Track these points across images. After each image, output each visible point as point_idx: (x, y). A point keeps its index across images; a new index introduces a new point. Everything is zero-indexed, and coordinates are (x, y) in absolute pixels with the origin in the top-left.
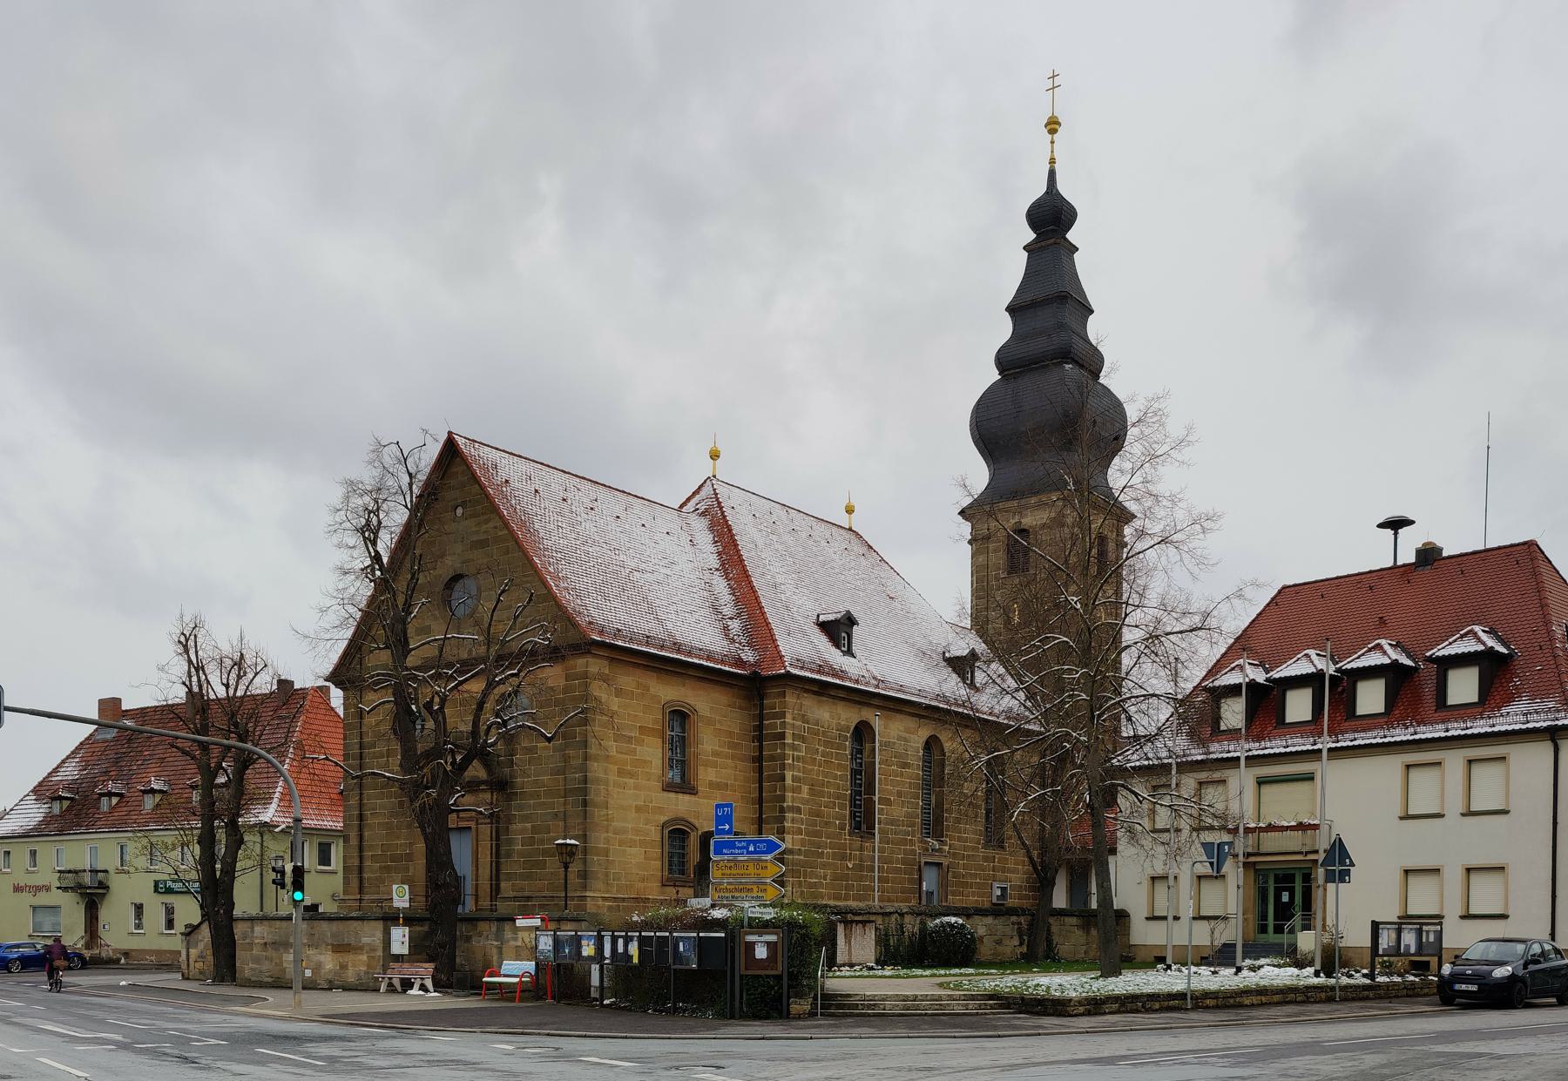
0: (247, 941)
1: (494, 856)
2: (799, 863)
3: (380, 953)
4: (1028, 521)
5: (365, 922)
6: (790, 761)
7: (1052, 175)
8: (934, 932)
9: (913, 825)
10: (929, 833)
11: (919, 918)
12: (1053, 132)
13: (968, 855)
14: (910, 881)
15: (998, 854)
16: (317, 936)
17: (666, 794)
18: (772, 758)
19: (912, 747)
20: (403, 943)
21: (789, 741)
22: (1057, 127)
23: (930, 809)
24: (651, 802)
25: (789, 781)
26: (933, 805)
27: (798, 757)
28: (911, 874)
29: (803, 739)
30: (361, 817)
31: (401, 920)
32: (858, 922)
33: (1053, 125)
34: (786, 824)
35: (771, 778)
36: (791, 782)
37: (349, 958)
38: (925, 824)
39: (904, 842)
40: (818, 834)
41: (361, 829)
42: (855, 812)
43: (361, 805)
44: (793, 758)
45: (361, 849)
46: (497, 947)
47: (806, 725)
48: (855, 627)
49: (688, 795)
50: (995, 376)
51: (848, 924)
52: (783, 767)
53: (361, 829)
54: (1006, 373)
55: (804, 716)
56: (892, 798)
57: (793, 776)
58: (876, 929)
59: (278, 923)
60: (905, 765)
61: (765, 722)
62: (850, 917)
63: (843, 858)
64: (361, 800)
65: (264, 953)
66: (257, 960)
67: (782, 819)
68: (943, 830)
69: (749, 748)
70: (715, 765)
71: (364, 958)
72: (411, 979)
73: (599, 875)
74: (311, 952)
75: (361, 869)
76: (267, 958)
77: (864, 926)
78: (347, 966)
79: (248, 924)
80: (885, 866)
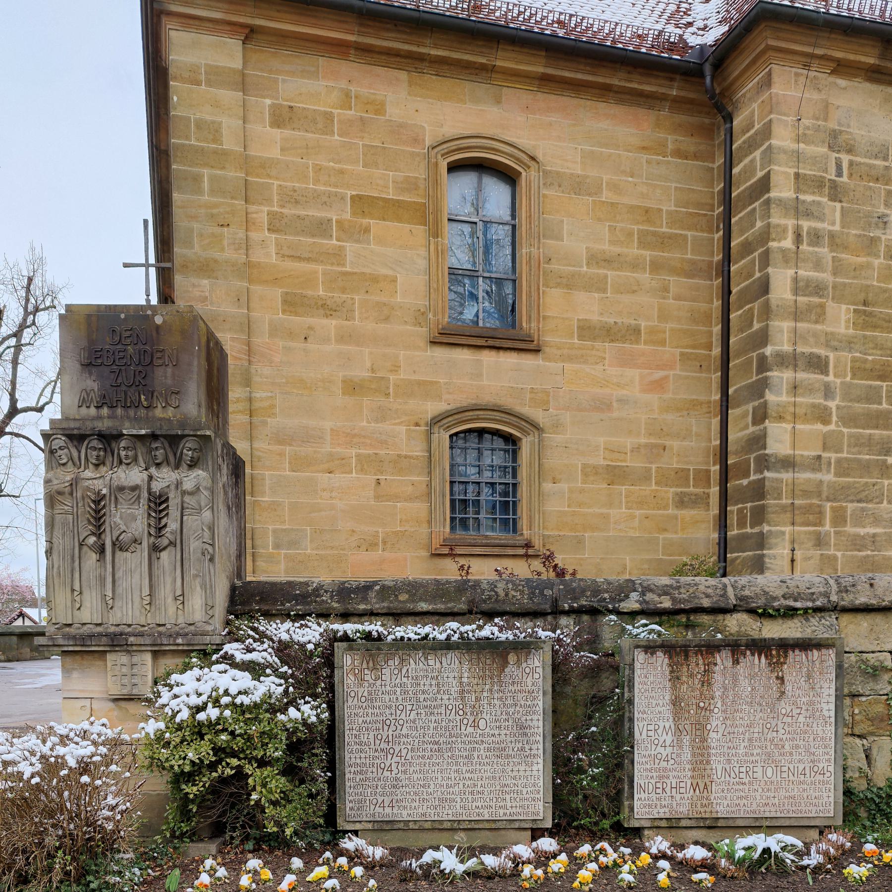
2: (817, 490)
6: (788, 243)
24: (395, 369)
27: (816, 237)
29: (836, 193)
32: (760, 647)
36: (789, 296)
47: (845, 158)
55: (834, 134)
57: (796, 280)
67: (759, 388)
70: (598, 285)
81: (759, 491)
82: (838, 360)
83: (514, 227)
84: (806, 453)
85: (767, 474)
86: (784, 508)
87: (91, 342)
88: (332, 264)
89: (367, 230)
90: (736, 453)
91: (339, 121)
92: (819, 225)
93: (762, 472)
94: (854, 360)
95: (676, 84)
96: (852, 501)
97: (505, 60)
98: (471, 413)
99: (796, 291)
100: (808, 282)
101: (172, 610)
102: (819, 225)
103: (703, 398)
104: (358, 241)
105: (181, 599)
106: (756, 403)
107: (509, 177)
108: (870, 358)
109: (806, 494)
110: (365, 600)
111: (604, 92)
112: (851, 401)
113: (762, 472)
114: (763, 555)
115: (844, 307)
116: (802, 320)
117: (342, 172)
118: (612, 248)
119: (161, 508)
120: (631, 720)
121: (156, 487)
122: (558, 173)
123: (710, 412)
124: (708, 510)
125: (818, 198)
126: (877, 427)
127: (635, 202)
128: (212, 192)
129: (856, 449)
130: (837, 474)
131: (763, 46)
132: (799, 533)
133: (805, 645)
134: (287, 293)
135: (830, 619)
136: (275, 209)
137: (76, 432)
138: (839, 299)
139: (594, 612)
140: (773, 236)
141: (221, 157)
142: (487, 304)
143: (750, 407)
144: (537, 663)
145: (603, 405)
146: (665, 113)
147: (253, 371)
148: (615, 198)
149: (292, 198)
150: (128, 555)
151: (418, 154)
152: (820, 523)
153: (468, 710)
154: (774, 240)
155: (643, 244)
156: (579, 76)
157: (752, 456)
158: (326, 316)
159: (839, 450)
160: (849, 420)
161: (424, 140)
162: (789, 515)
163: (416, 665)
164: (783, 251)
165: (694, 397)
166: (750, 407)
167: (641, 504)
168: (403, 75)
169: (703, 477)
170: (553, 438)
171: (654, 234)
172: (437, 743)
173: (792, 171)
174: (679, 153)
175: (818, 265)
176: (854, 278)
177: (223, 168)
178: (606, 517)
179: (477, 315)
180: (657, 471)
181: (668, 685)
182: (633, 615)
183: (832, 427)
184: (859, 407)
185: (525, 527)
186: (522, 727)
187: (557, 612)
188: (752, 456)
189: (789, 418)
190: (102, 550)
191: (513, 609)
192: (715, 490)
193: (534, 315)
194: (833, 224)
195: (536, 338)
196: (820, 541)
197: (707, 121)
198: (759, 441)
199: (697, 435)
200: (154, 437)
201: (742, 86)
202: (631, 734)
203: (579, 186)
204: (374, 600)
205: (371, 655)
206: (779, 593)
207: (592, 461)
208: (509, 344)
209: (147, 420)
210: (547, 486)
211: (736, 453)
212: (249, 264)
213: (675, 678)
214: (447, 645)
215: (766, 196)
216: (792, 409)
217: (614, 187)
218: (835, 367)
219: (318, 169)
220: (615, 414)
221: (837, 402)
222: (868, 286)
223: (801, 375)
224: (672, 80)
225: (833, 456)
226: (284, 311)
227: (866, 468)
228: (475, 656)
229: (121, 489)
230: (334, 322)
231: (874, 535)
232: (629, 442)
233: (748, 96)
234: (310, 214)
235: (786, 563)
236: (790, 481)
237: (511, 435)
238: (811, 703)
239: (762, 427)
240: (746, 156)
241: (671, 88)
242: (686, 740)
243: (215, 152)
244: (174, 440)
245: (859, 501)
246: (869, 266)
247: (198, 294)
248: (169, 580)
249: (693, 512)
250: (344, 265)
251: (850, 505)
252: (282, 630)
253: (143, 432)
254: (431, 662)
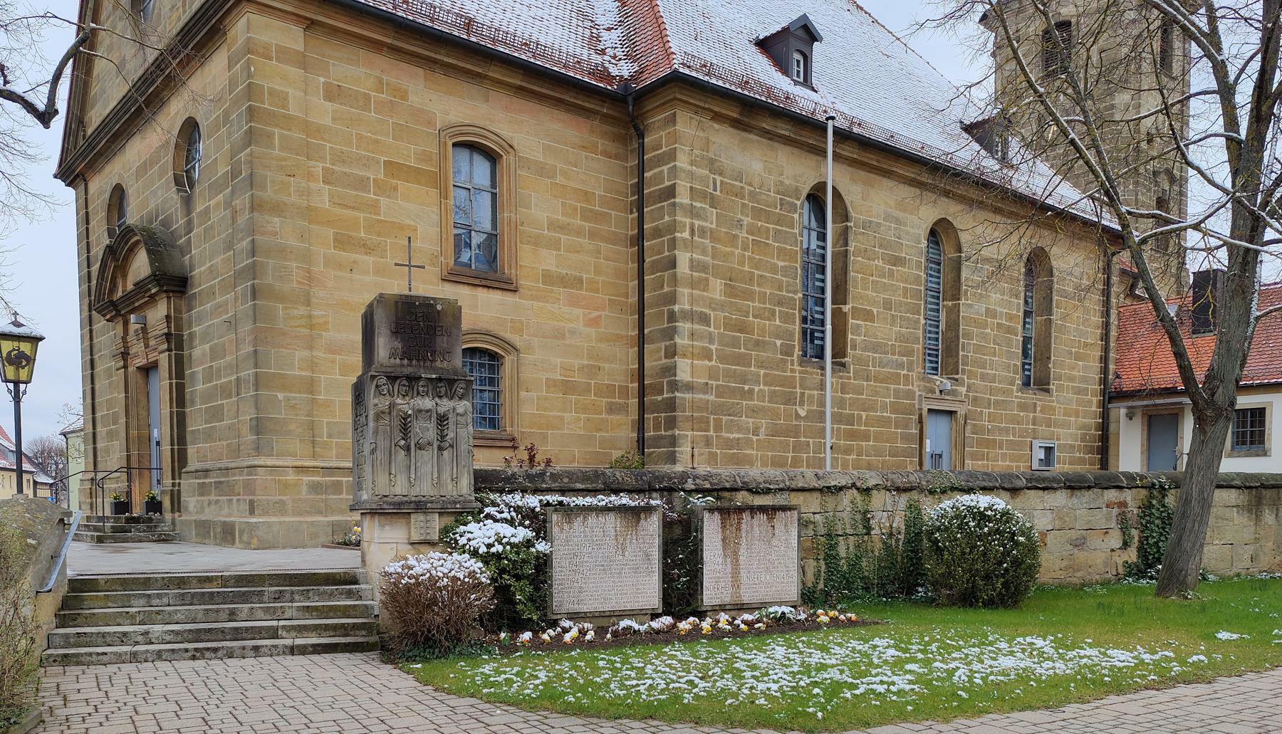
2: (704, 407)
6: (686, 235)
8: (938, 529)
9: (909, 353)
10: (936, 369)
11: (903, 500)
13: (997, 402)
14: (906, 438)
15: (1040, 400)
19: (908, 233)
21: (683, 198)
23: (937, 333)
25: (683, 267)
26: (942, 325)
27: (703, 232)
28: (906, 426)
32: (754, 510)
34: (678, 340)
35: (656, 267)
36: (687, 271)
38: (929, 355)
39: (895, 378)
40: (742, 360)
42: (813, 332)
44: (692, 231)
49: (499, 292)
51: (727, 512)
52: (673, 243)
56: (875, 311)
57: (691, 260)
58: (803, 524)
60: (898, 261)
61: (645, 175)
62: (741, 498)
63: (789, 400)
67: (670, 333)
68: (957, 362)
69: (623, 223)
70: (555, 245)
73: (292, 427)
77: (771, 519)
80: (864, 414)
81: (671, 405)
82: (716, 317)
83: (494, 195)
84: (699, 381)
85: (677, 394)
86: (687, 417)
87: (397, 318)
88: (371, 213)
89: (396, 189)
90: (652, 376)
91: (375, 102)
92: (704, 224)
93: (673, 393)
94: (725, 318)
95: (606, 105)
96: (725, 415)
97: (495, 73)
98: (471, 336)
99: (692, 268)
100: (699, 262)
101: (450, 487)
102: (704, 224)
103: (624, 333)
104: (389, 197)
105: (455, 480)
106: (668, 343)
107: (492, 157)
108: (734, 317)
109: (700, 409)
110: (544, 481)
111: (558, 103)
112: (723, 346)
113: (673, 393)
114: (675, 451)
115: (719, 281)
116: (696, 289)
117: (377, 141)
118: (564, 219)
119: (445, 423)
120: (702, 550)
121: (441, 410)
122: (528, 159)
123: (628, 344)
124: (627, 416)
125: (703, 206)
126: (738, 365)
127: (578, 187)
128: (282, 148)
129: (726, 379)
130: (716, 396)
131: (672, 97)
132: (696, 435)
133: (784, 509)
134: (337, 233)
135: (786, 495)
136: (328, 165)
137: (393, 375)
138: (716, 276)
139: (671, 490)
140: (678, 229)
141: (288, 121)
142: (477, 251)
143: (663, 345)
144: (655, 519)
145: (559, 335)
146: (596, 123)
147: (312, 294)
148: (565, 182)
149: (340, 158)
150: (423, 452)
151: (432, 134)
152: (708, 430)
153: (620, 546)
154: (678, 232)
155: (584, 218)
156: (544, 91)
157: (665, 380)
158: (366, 254)
159: (718, 380)
160: (723, 358)
161: (436, 123)
162: (690, 423)
163: (592, 520)
164: (684, 240)
165: (618, 332)
166: (663, 345)
167: (585, 410)
168: (420, 71)
169: (624, 392)
170: (527, 358)
171: (591, 210)
172: (603, 566)
173: (688, 185)
174: (606, 154)
175: (704, 252)
176: (724, 262)
177: (289, 130)
178: (562, 419)
179: (470, 260)
180: (594, 386)
181: (720, 530)
182: (690, 492)
183: (713, 363)
184: (729, 350)
185: (507, 425)
186: (647, 555)
187: (652, 489)
188: (665, 380)
189: (689, 355)
190: (408, 449)
191: (629, 488)
192: (634, 402)
193: (513, 264)
194: (712, 223)
195: (515, 282)
196: (708, 442)
197: (623, 132)
198: (670, 370)
199: (620, 360)
200: (440, 380)
201: (652, 117)
202: (702, 558)
203: (542, 171)
204: (550, 482)
205: (568, 515)
206: (761, 480)
207: (552, 376)
208: (497, 285)
209: (434, 370)
210: (523, 394)
211: (652, 376)
212: (309, 208)
213: (724, 527)
214: (606, 509)
215: (673, 200)
216: (691, 350)
217: (564, 174)
218: (714, 322)
219: (360, 138)
220: (568, 342)
221: (715, 346)
222: (732, 268)
223: (696, 326)
224: (605, 102)
225: (714, 383)
226: (335, 248)
227: (733, 392)
228: (623, 515)
229: (420, 411)
230: (372, 259)
231: (738, 439)
232: (576, 363)
233: (657, 124)
234: (354, 172)
235: (690, 455)
236: (691, 400)
237: (496, 353)
238: (786, 540)
239: (672, 360)
240: (656, 167)
241: (603, 107)
242: (729, 560)
243: (284, 116)
244: (451, 382)
245: (729, 415)
246: (733, 253)
247: (271, 229)
248: (448, 468)
249: (618, 417)
250: (379, 215)
251: (724, 418)
252: (517, 499)
253: (434, 376)
254: (600, 518)
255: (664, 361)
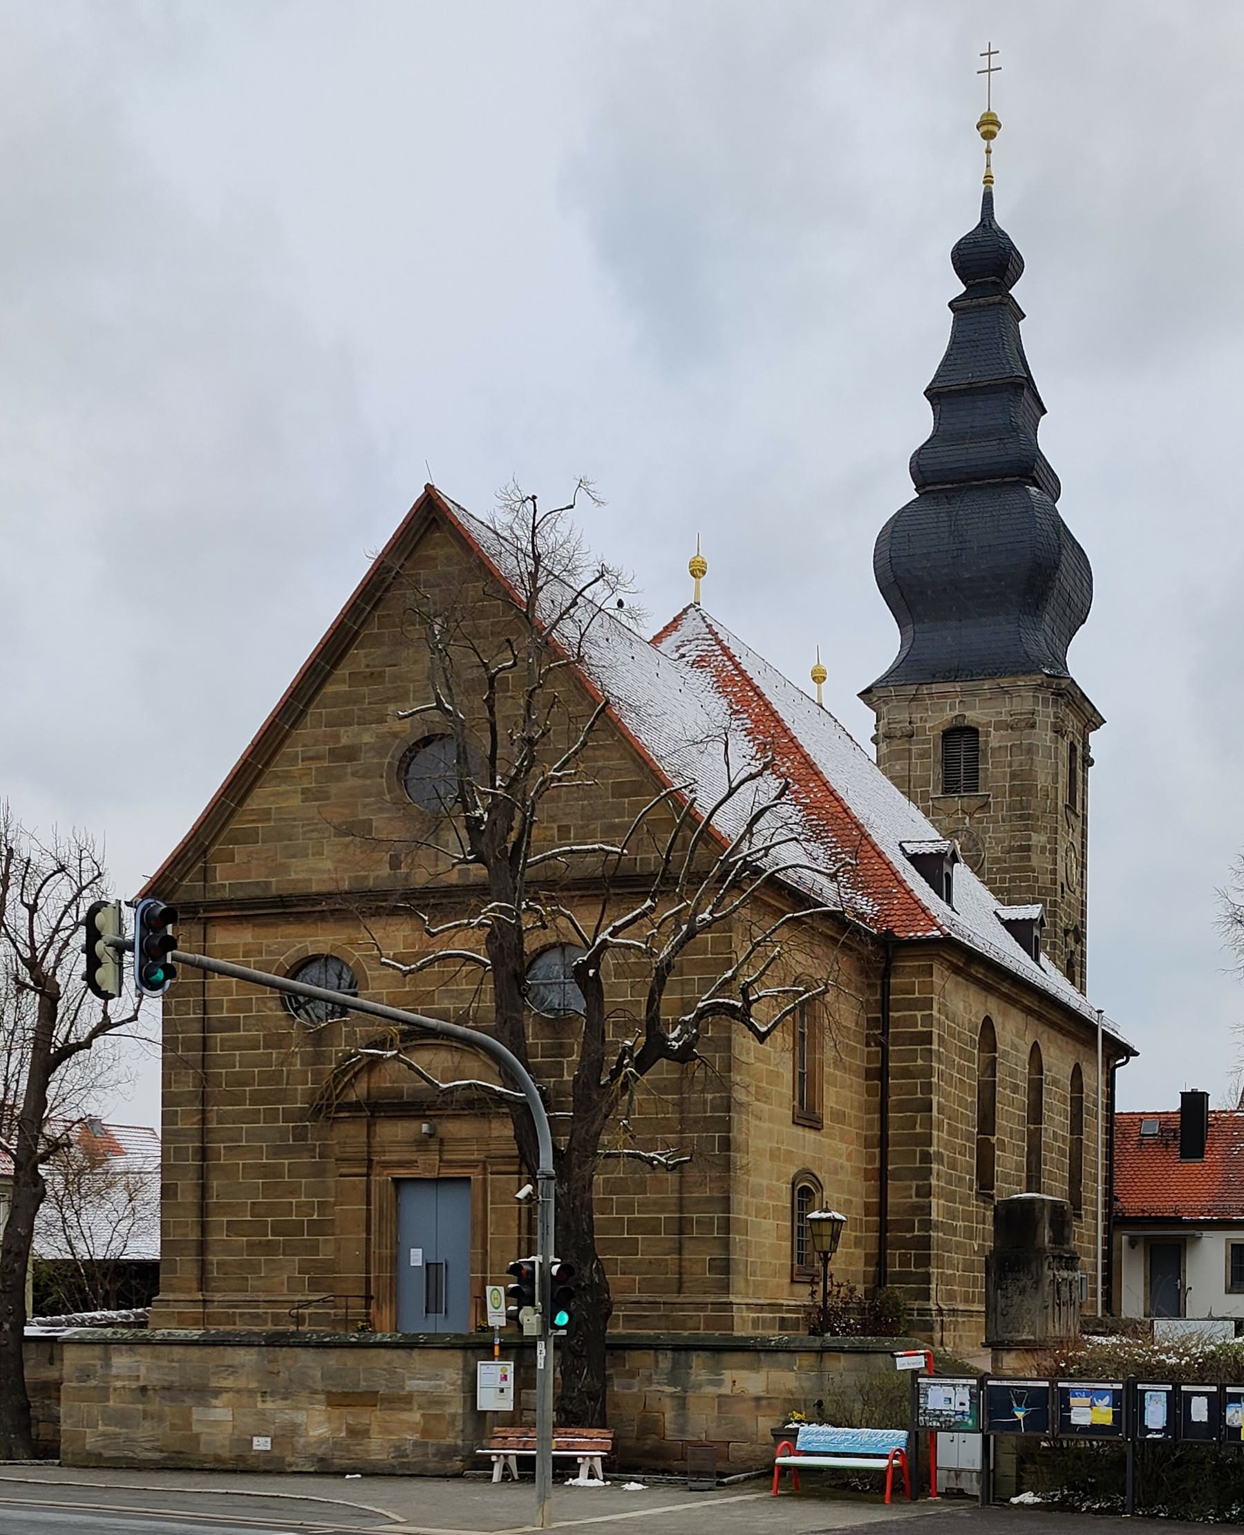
0: (93, 1383)
1: (524, 1230)
3: (456, 1408)
4: (974, 716)
5: (416, 1353)
7: (988, 200)
12: (988, 136)
16: (284, 1375)
17: (800, 1131)
18: (906, 1073)
20: (502, 1391)
22: (995, 128)
30: (203, 1153)
31: (497, 1349)
33: (989, 127)
35: (902, 1106)
37: (371, 1418)
41: (203, 1173)
43: (204, 1133)
45: (203, 1209)
46: (672, 1396)
48: (956, 865)
50: (909, 493)
53: (203, 1173)
54: (928, 488)
59: (178, 1351)
64: (204, 1121)
65: (140, 1407)
66: (122, 1419)
71: (416, 1416)
72: (576, 1457)
74: (269, 1405)
75: (202, 1247)
76: (146, 1415)
78: (367, 1431)
79: (98, 1351)
106: (921, 1183)
239: (927, 1200)
255: (915, 1199)
